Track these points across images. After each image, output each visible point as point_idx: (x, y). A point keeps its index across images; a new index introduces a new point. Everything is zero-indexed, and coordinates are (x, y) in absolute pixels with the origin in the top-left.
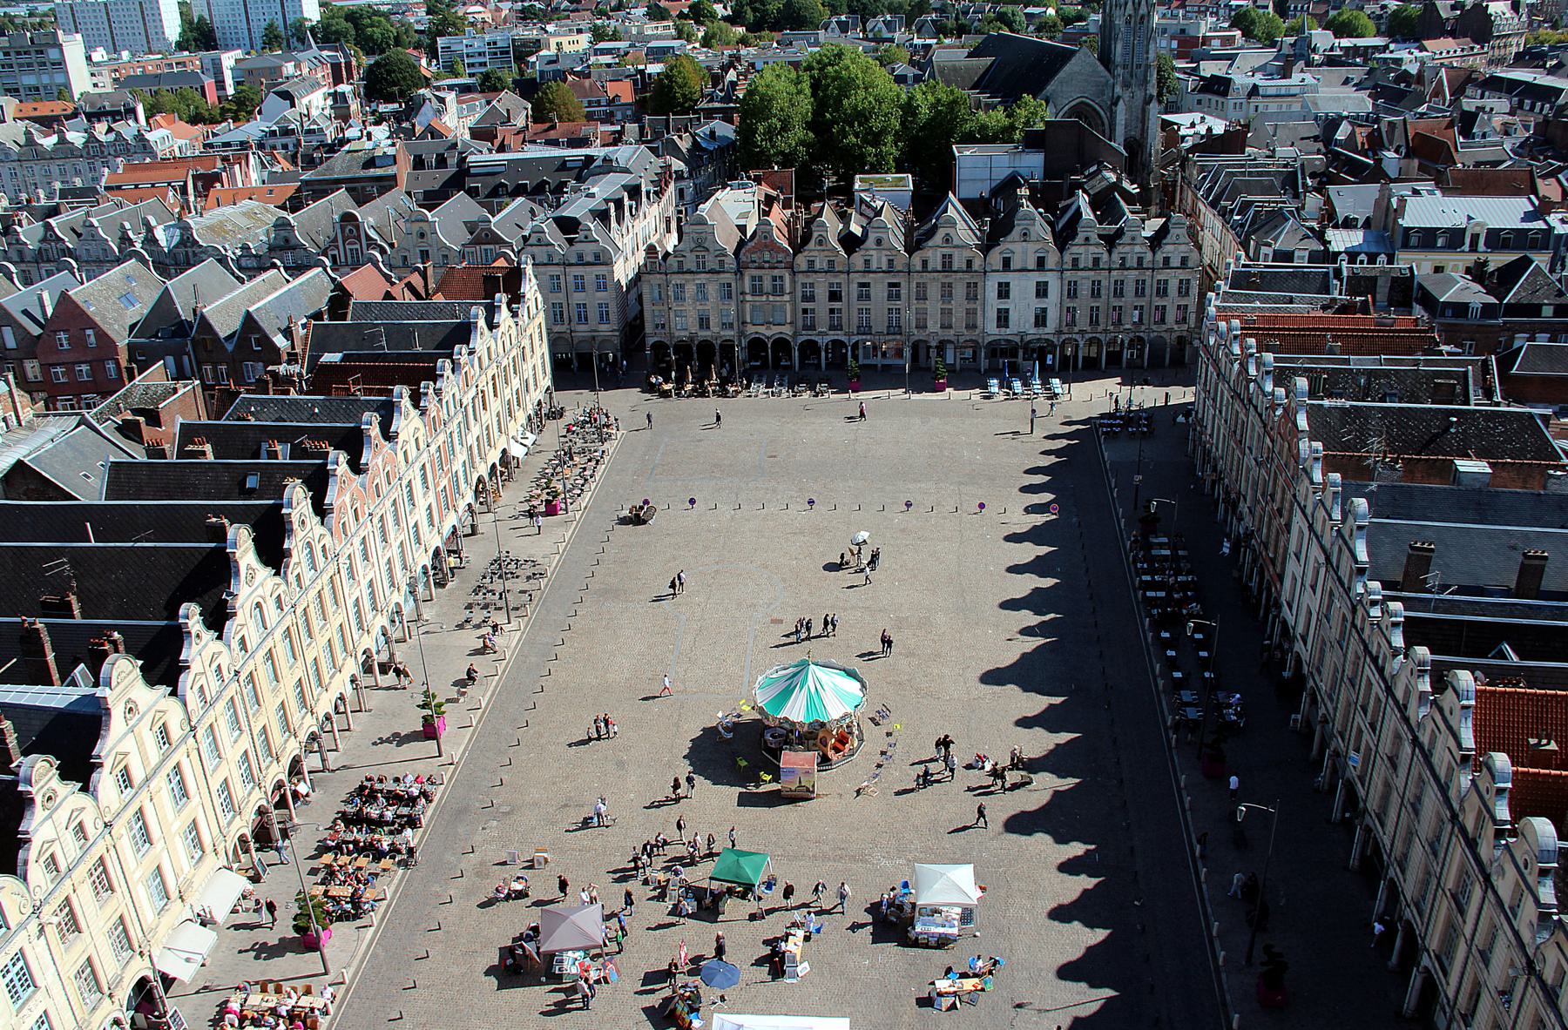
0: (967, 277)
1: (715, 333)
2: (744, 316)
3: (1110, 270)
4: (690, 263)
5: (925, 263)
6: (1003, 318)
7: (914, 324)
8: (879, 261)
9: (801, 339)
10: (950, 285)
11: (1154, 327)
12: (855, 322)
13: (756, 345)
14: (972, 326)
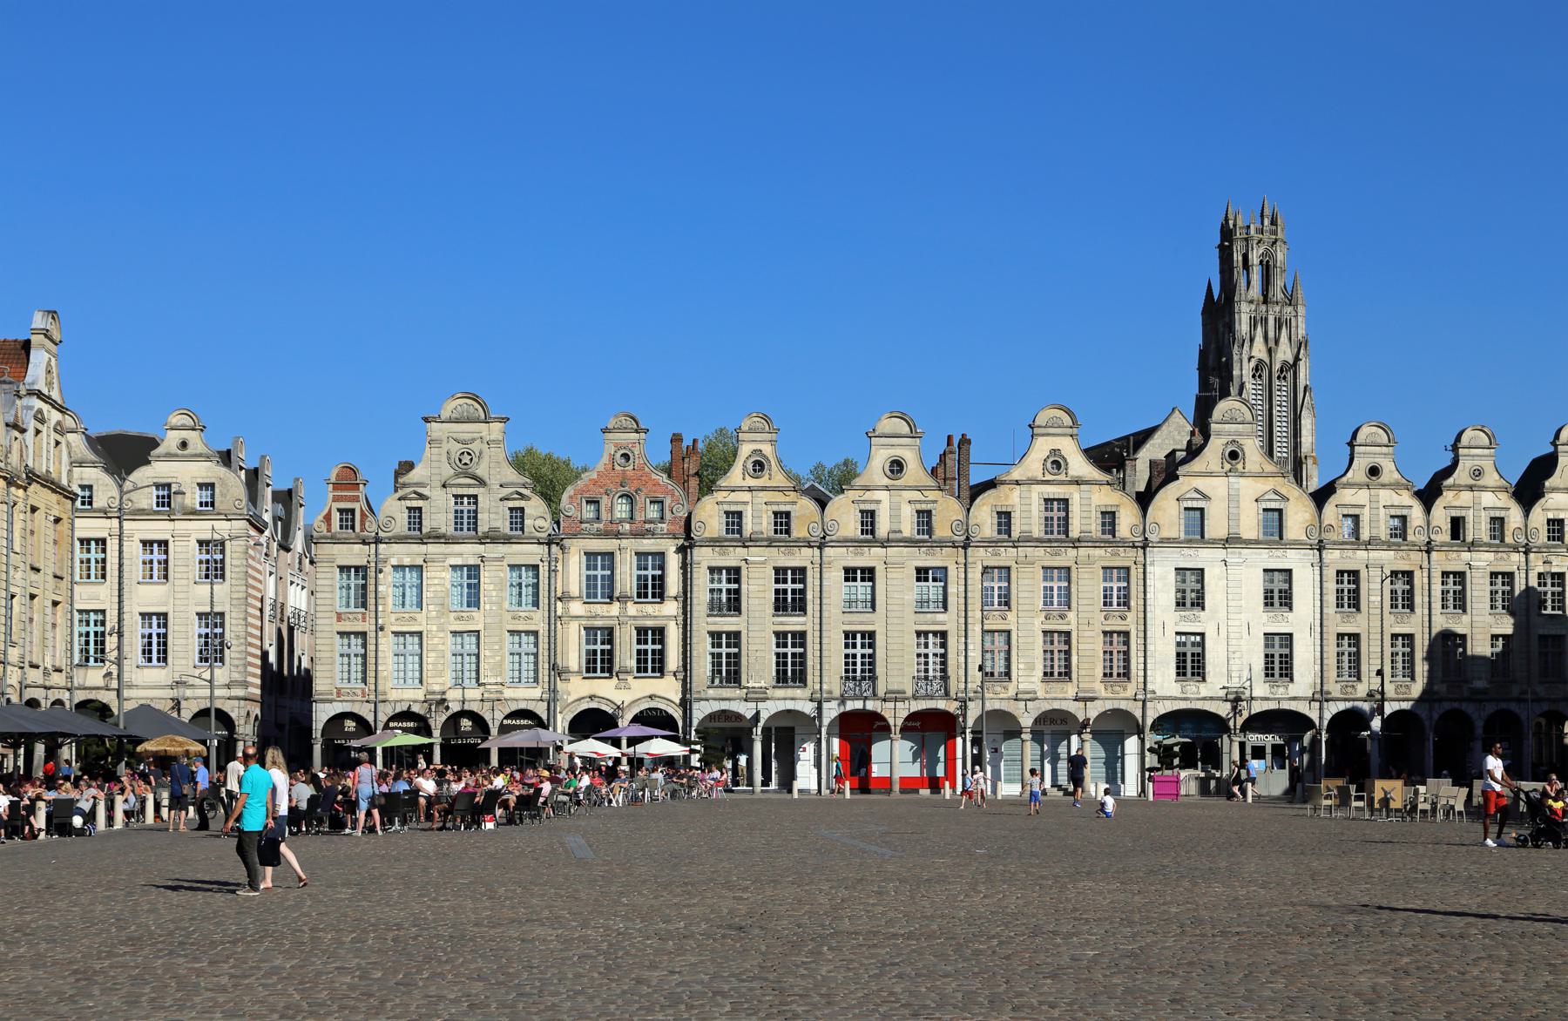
3: (1429, 548)
4: (439, 515)
5: (1005, 518)
6: (1191, 663)
9: (700, 712)
11: (1541, 690)
14: (1119, 669)
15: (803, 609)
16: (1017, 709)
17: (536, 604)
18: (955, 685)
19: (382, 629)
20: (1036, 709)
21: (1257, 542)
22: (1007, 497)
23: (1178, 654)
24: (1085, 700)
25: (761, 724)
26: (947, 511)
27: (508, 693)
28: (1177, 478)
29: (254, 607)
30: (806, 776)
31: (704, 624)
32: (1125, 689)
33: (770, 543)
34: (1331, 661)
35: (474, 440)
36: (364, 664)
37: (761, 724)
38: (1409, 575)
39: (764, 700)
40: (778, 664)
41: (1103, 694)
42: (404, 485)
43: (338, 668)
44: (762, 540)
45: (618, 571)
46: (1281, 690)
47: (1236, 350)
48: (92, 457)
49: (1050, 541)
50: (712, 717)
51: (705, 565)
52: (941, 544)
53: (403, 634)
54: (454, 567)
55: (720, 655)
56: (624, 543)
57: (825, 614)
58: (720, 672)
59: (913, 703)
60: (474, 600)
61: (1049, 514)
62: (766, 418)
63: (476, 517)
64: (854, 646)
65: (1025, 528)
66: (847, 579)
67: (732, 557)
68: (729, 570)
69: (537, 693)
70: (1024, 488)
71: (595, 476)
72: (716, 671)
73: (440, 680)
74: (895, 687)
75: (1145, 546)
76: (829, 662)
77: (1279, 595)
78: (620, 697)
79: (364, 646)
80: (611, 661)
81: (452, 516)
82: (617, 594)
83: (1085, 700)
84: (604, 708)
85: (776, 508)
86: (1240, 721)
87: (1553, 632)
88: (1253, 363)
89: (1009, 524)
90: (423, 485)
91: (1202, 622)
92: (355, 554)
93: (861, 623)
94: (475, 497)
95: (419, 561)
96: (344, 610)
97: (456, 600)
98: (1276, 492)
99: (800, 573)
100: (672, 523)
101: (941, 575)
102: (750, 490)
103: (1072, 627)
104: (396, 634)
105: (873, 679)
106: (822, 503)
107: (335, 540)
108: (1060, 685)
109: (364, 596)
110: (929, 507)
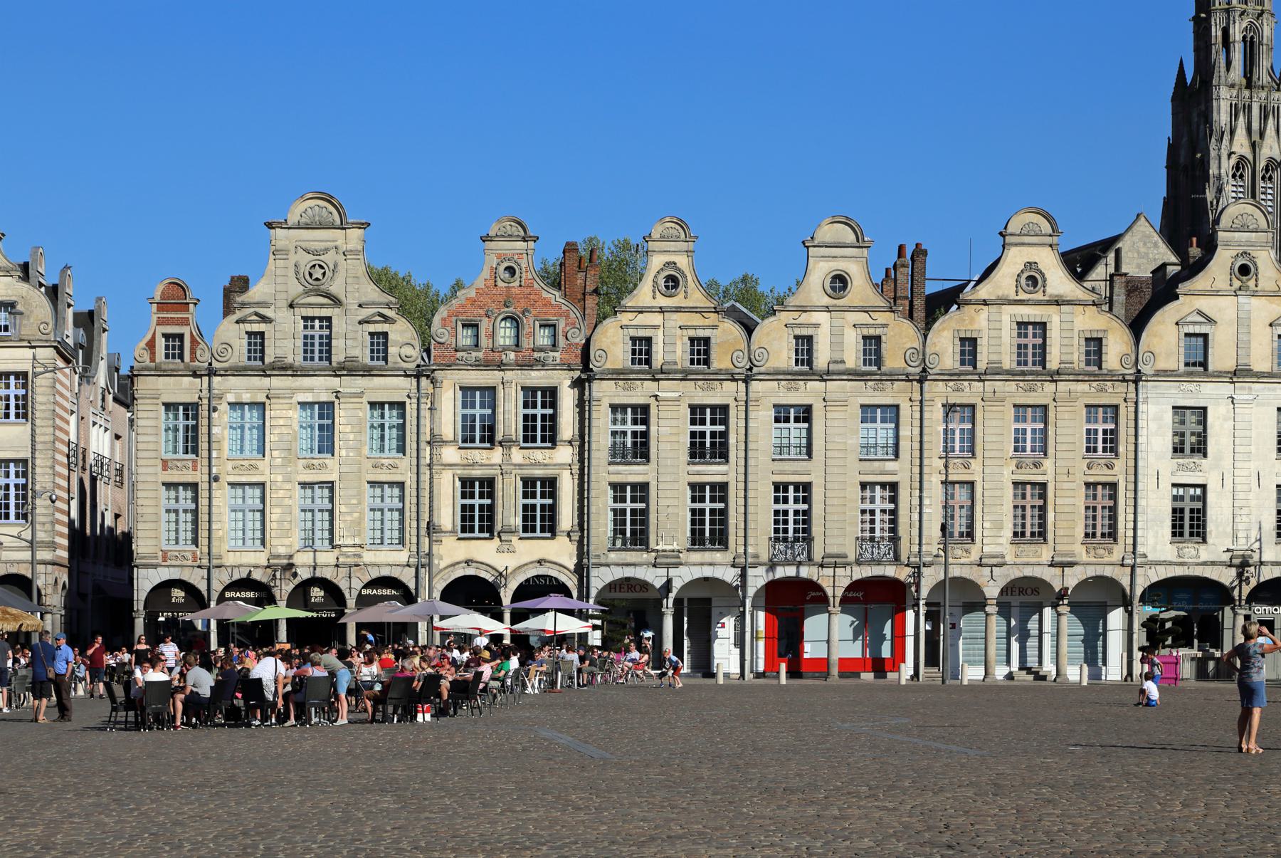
0: (1085, 391)
4: (285, 341)
5: (969, 346)
6: (1190, 520)
8: (837, 343)
9: (599, 579)
14: (1103, 528)
15: (724, 456)
16: (980, 576)
17: (402, 449)
19: (216, 479)
22: (972, 320)
23: (1174, 511)
24: (1063, 565)
25: (672, 595)
26: (900, 337)
27: (368, 557)
28: (1176, 297)
29: (61, 452)
30: (725, 657)
31: (604, 473)
32: (1110, 552)
33: (685, 376)
35: (327, 250)
36: (195, 522)
40: (693, 522)
41: (1085, 558)
42: (243, 305)
43: (164, 526)
44: (676, 372)
45: (500, 410)
47: (1213, 144)
49: (1023, 373)
50: (612, 586)
52: (892, 377)
53: (242, 485)
54: (303, 405)
56: (509, 375)
57: (751, 462)
58: (623, 532)
59: (856, 569)
60: (327, 444)
61: (1023, 341)
62: (681, 224)
63: (329, 344)
64: (786, 500)
65: (994, 358)
66: (777, 420)
67: (640, 393)
68: (635, 408)
69: (403, 557)
70: (993, 309)
71: (473, 294)
72: (619, 530)
73: (287, 541)
76: (755, 521)
78: (502, 561)
79: (195, 500)
80: (491, 519)
81: (300, 343)
82: (499, 437)
83: (1063, 565)
84: (483, 575)
85: (692, 333)
86: (1246, 590)
88: (1233, 161)
89: (974, 353)
90: (265, 305)
91: (1206, 472)
92: (184, 389)
94: (329, 319)
95: (261, 398)
96: (170, 456)
97: (306, 444)
99: (721, 412)
100: (565, 351)
101: (893, 412)
102: (662, 311)
103: (1049, 478)
104: (233, 485)
105: (809, 540)
106: (749, 329)
107: (160, 372)
108: (1033, 547)
109: (195, 439)
110: (878, 332)
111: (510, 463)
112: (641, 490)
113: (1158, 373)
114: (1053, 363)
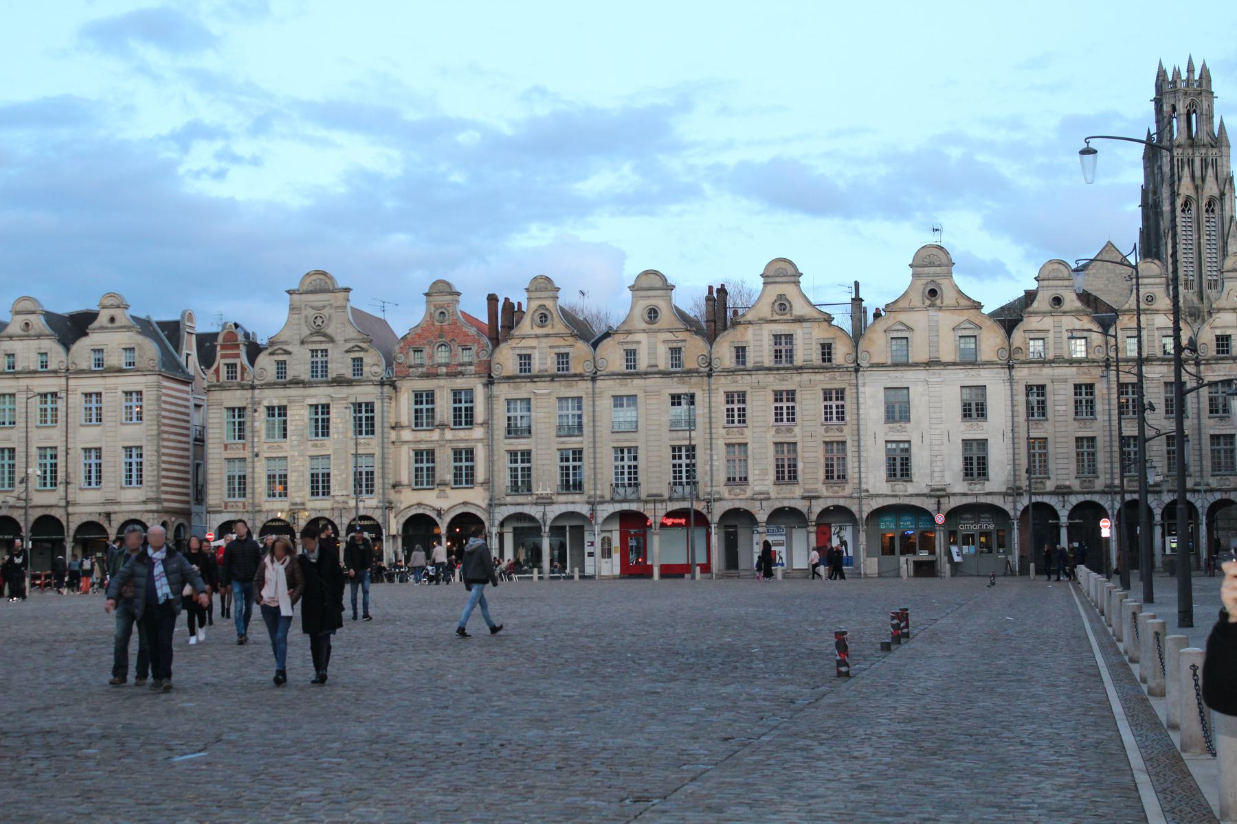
0: (824, 380)
1: (341, 504)
2: (397, 471)
4: (299, 366)
5: (741, 352)
6: (899, 466)
7: (721, 477)
8: (652, 352)
9: (502, 513)
10: (791, 396)
11: (1214, 482)
12: (608, 474)
13: (419, 529)
14: (835, 474)
16: (754, 508)
18: (703, 489)
19: (257, 455)
20: (769, 507)
21: (954, 364)
26: (694, 348)
33: (553, 378)
34: (1024, 463)
35: (324, 307)
37: (549, 523)
38: (1090, 387)
39: (552, 503)
46: (978, 487)
48: (48, 331)
49: (778, 369)
51: (502, 398)
53: (274, 458)
55: (516, 469)
56: (442, 382)
61: (778, 347)
65: (758, 359)
66: (615, 406)
67: (525, 390)
70: (757, 327)
73: (301, 494)
74: (654, 492)
75: (857, 371)
76: (601, 472)
77: (974, 409)
78: (443, 504)
80: (433, 476)
81: (309, 366)
82: (437, 422)
83: (810, 498)
84: (428, 513)
85: (557, 351)
87: (1224, 432)
89: (744, 357)
91: (910, 432)
92: (236, 398)
93: (626, 440)
94: (326, 350)
95: (284, 403)
98: (970, 322)
102: (537, 337)
104: (269, 459)
105: (637, 485)
107: (222, 387)
108: (789, 487)
110: (679, 345)
111: (444, 440)
112: (527, 455)
113: (873, 366)
114: (799, 360)
